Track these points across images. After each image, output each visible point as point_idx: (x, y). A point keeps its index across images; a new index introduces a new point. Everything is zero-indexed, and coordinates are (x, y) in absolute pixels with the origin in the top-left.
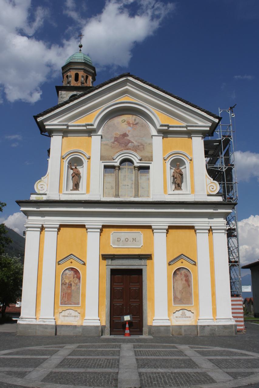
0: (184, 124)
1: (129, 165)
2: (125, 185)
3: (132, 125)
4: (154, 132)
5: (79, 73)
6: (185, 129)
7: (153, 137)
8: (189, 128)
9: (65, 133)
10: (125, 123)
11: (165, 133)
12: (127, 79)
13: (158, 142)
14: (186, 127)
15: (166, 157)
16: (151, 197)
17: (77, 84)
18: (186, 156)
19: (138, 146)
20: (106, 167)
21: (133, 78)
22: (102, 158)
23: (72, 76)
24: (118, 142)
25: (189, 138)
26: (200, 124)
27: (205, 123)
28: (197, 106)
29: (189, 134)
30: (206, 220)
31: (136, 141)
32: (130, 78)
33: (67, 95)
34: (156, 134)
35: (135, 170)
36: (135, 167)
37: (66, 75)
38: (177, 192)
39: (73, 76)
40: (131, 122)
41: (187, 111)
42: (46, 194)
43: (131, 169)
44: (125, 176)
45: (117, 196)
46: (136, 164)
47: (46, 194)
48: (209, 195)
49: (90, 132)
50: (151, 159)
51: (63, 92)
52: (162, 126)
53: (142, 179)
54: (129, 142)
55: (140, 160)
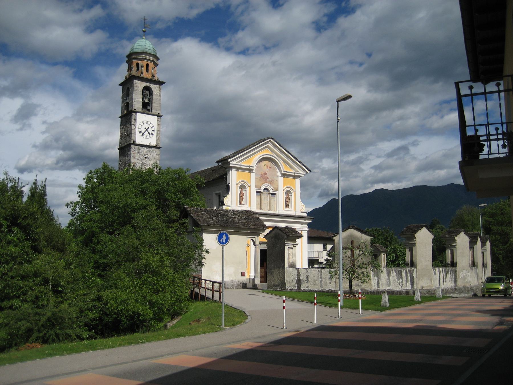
0: (294, 172)
1: (266, 192)
2: (265, 203)
3: (268, 168)
4: (279, 174)
5: (149, 64)
6: (293, 174)
7: (279, 177)
8: (296, 174)
9: (238, 169)
10: (266, 166)
11: (284, 175)
12: (270, 140)
13: (281, 179)
14: (294, 173)
15: (284, 189)
16: (277, 211)
17: (148, 75)
18: (292, 189)
19: (272, 181)
20: (257, 192)
21: (274, 140)
22: (256, 187)
23: (144, 66)
24: (263, 178)
25: (294, 179)
26: (301, 172)
27: (302, 172)
28: (301, 163)
29: (294, 177)
30: (300, 225)
31: (270, 178)
32: (272, 140)
33: (141, 85)
34: (280, 175)
35: (269, 195)
36: (269, 193)
37: (136, 62)
38: (287, 209)
39: (145, 66)
40: (268, 166)
41: (292, 161)
42: (230, 206)
43: (267, 194)
44: (264, 198)
45: (261, 209)
46: (271, 192)
47: (230, 206)
48: (302, 212)
49: (250, 170)
50: (277, 189)
51: (138, 82)
52: (284, 171)
53: (273, 200)
54: (268, 178)
55: (273, 190)
